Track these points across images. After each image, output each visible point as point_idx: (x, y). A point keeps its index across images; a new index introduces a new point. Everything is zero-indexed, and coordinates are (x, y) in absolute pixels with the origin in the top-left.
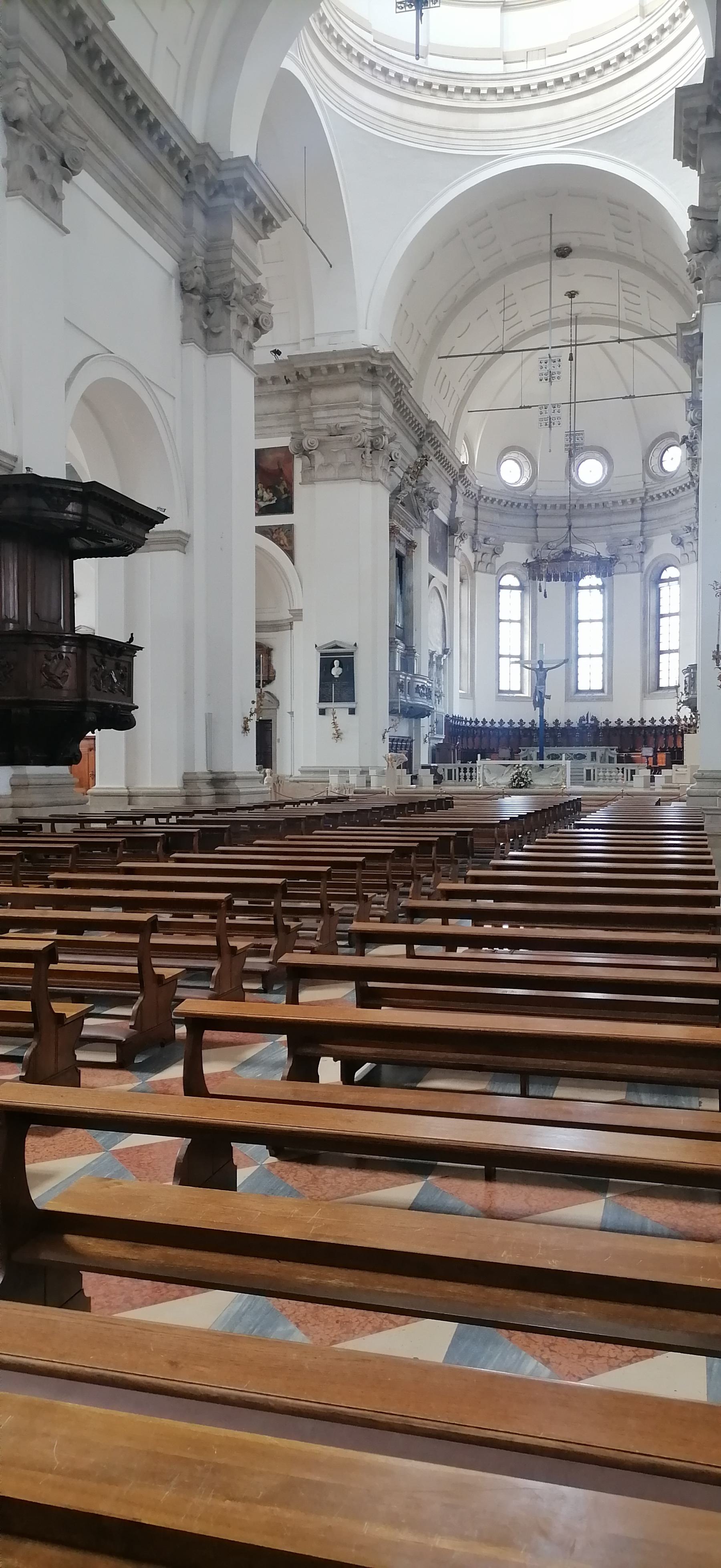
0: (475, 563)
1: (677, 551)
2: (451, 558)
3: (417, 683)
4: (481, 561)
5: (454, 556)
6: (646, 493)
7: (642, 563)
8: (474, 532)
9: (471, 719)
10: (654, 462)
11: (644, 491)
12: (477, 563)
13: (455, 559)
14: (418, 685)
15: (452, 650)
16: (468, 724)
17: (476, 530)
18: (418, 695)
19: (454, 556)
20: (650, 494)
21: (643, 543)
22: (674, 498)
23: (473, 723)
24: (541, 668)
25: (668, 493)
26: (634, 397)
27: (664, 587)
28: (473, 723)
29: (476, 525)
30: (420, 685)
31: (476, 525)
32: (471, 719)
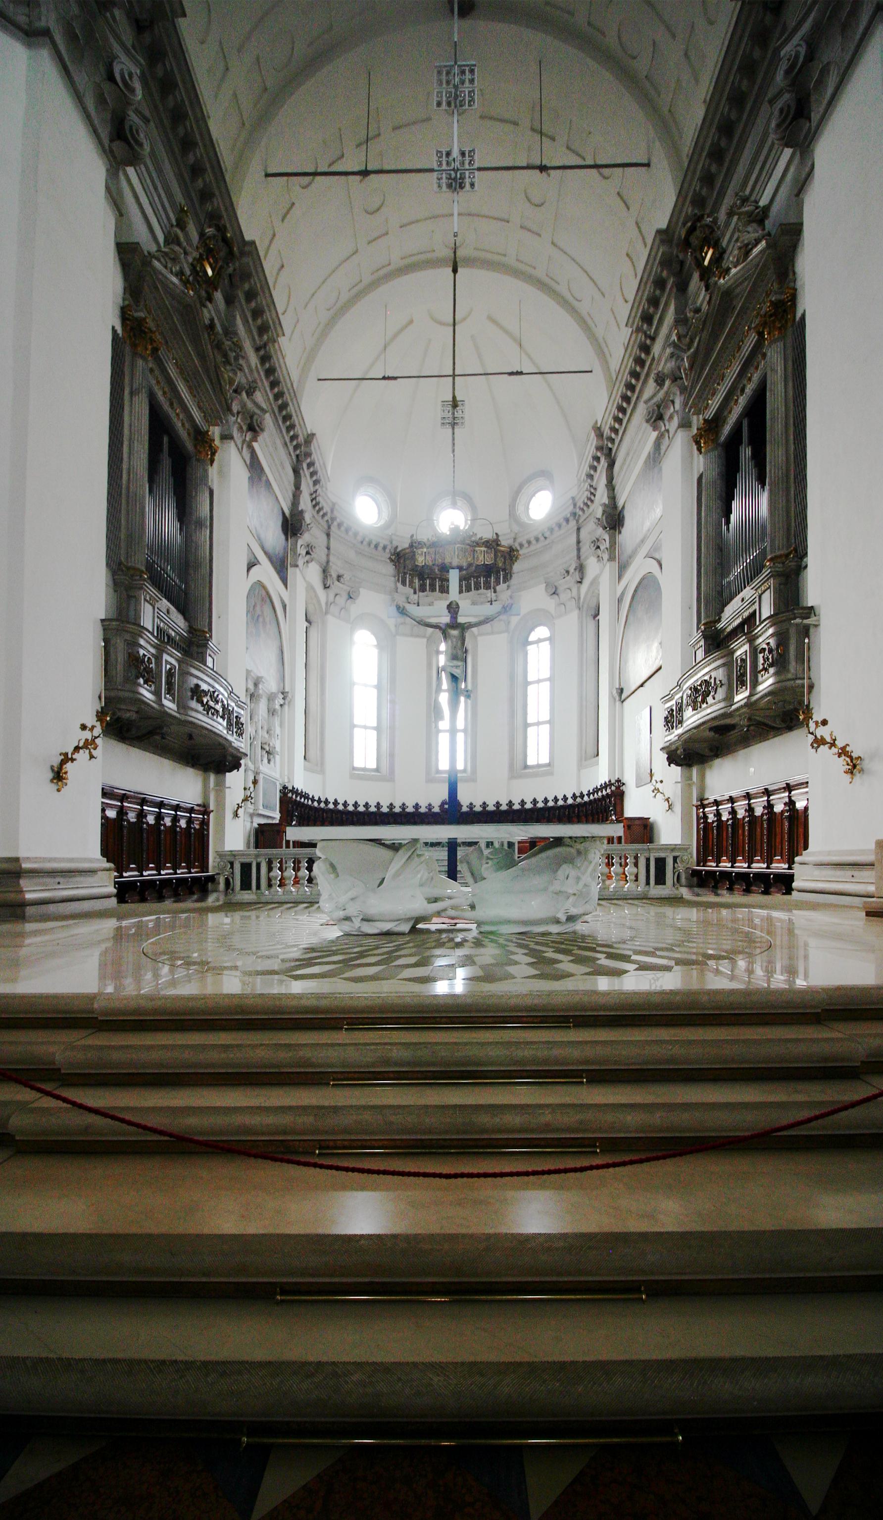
1: (550, 604)
3: (195, 681)
6: (515, 539)
7: (509, 623)
10: (520, 510)
11: (513, 535)
14: (197, 686)
18: (194, 704)
20: (519, 540)
21: (511, 597)
22: (547, 542)
24: (454, 624)
25: (540, 536)
26: (521, 373)
27: (531, 649)
30: (204, 687)
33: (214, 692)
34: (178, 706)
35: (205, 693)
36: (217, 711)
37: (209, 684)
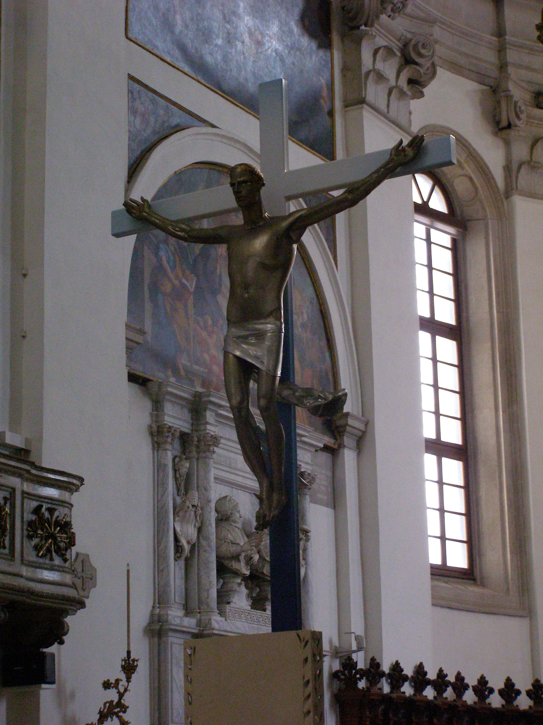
0: (507, 168)
2: (353, 112)
4: (529, 162)
5: (362, 101)
8: (494, 72)
9: (509, 683)
12: (515, 166)
13: (367, 115)
15: (368, 423)
16: (449, 694)
17: (503, 66)
19: (362, 101)
23: (450, 689)
28: (450, 689)
29: (501, 50)
31: (501, 50)
32: (509, 683)
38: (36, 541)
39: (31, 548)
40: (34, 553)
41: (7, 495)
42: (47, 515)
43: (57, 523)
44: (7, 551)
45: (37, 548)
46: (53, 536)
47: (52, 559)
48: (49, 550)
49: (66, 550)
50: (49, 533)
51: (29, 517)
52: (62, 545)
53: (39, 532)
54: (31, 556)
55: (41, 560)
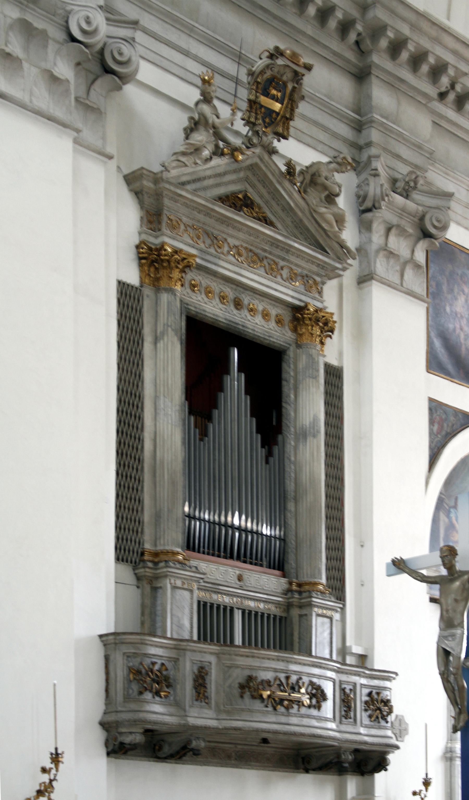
30: (269, 676)
33: (288, 678)
34: (218, 711)
35: (268, 684)
36: (300, 703)
37: (276, 670)
38: (369, 712)
39: (366, 717)
40: (368, 719)
41: (351, 687)
42: (376, 696)
43: (382, 701)
44: (352, 720)
45: (370, 716)
46: (379, 709)
47: (379, 722)
48: (377, 717)
49: (387, 716)
50: (377, 707)
51: (366, 698)
52: (385, 713)
53: (372, 707)
54: (366, 721)
55: (372, 723)
